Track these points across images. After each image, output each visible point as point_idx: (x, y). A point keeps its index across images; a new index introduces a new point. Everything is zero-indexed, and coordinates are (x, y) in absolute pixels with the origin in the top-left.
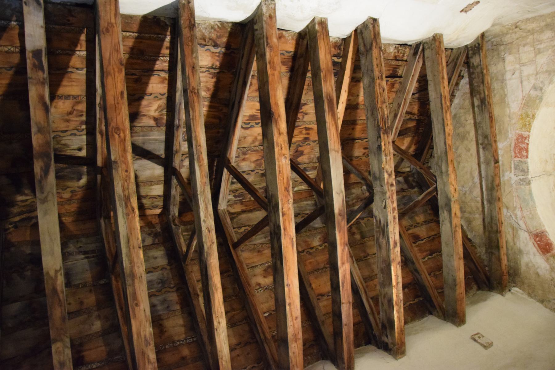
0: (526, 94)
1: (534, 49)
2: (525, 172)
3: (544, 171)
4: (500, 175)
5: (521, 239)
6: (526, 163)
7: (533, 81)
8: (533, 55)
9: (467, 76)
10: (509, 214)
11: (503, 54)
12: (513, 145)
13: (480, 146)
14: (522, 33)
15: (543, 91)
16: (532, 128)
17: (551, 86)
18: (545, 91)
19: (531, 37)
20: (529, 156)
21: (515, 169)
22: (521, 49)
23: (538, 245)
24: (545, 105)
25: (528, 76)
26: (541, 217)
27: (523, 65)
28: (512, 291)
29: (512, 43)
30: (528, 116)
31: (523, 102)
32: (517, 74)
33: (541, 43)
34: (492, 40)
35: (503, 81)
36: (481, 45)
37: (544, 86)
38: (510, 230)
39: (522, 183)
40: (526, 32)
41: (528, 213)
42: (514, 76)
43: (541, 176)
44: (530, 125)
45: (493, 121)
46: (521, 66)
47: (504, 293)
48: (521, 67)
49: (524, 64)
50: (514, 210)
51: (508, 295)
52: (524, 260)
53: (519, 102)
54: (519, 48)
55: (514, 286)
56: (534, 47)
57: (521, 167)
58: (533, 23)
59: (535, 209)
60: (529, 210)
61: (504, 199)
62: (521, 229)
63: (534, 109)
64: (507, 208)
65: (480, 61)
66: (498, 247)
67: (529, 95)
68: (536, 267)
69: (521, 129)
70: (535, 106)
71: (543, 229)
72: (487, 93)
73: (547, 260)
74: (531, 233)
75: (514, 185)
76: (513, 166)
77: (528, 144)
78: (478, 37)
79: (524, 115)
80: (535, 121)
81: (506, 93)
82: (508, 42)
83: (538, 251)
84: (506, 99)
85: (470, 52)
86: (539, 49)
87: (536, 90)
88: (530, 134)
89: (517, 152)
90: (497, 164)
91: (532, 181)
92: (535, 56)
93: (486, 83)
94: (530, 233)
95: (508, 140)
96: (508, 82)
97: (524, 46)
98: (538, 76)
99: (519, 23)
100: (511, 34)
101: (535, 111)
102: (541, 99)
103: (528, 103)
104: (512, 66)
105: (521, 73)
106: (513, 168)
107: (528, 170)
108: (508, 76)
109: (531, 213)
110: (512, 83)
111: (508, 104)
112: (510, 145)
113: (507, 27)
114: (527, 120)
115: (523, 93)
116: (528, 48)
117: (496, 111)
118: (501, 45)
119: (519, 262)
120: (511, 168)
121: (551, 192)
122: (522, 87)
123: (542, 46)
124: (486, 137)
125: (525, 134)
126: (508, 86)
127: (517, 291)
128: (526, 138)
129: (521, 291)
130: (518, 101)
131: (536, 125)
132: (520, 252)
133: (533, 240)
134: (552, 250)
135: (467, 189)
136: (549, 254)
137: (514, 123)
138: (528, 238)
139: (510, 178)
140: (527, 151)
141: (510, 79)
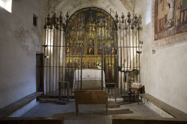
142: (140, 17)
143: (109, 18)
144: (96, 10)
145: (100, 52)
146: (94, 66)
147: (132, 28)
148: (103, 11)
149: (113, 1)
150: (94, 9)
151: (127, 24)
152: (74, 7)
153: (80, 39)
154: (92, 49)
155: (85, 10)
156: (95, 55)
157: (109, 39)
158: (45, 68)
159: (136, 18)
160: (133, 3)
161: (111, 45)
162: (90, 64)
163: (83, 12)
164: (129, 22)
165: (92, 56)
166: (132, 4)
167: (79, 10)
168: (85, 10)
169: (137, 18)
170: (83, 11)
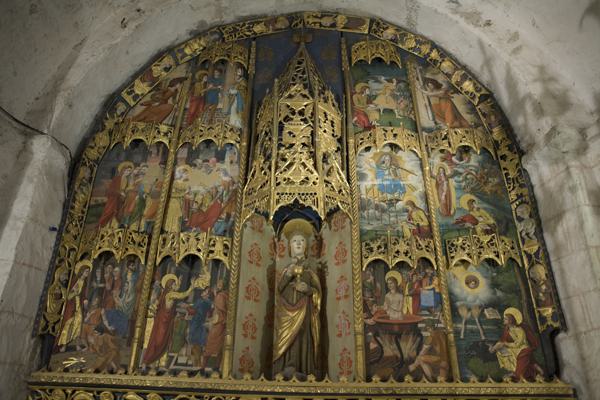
143: (441, 79)
144: (339, 28)
145: (389, 350)
153: (194, 219)
154: (307, 323)
157: (465, 224)
161: (494, 285)
168: (258, 29)
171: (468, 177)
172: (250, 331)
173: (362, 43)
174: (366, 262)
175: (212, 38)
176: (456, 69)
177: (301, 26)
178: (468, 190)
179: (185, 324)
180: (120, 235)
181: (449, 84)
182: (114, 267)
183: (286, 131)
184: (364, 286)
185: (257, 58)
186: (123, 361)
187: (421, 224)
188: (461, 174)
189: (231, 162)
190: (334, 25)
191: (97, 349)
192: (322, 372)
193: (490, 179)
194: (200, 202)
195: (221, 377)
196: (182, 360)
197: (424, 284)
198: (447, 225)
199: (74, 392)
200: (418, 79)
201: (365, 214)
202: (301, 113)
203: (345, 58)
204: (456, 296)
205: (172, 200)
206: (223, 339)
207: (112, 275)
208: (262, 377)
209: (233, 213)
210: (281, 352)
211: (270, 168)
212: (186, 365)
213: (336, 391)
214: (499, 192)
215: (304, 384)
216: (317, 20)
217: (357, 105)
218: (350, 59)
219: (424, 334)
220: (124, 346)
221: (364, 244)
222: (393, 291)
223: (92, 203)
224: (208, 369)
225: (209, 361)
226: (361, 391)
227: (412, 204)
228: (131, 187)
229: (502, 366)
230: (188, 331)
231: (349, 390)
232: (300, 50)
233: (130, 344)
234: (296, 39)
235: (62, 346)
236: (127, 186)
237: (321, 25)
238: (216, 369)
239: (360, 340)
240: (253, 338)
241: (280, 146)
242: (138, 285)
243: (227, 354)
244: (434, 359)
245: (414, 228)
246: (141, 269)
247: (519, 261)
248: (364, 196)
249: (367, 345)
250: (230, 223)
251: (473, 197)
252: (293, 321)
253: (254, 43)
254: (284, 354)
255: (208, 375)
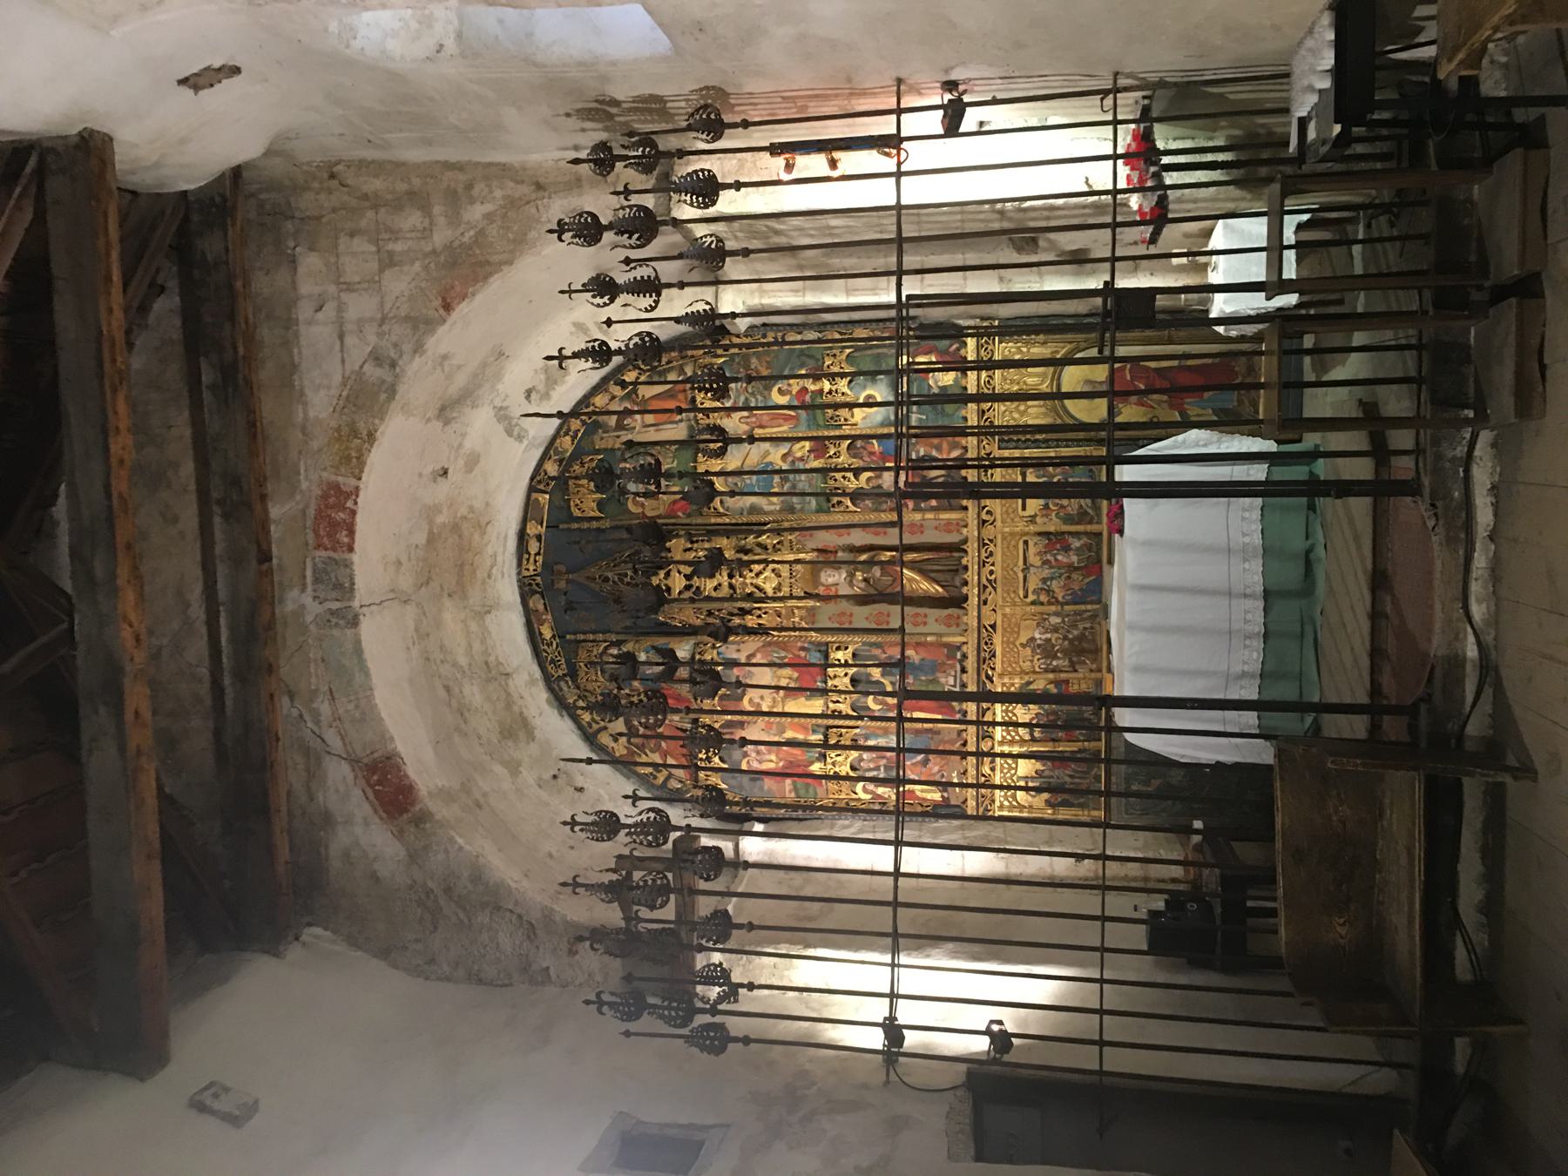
0: (352, 372)
1: (379, 251)
2: (345, 589)
3: (393, 591)
4: (273, 597)
5: (330, 783)
6: (348, 565)
7: (372, 339)
8: (375, 266)
9: (177, 290)
10: (295, 712)
11: (291, 244)
12: (311, 512)
13: (216, 509)
14: (346, 198)
15: (398, 370)
16: (366, 469)
17: (417, 359)
18: (403, 371)
19: (370, 214)
20: (357, 546)
21: (317, 581)
22: (343, 240)
23: (376, 793)
24: (402, 408)
25: (360, 323)
26: (384, 715)
27: (348, 290)
28: (304, 938)
29: (318, 218)
30: (355, 433)
31: (345, 394)
32: (329, 310)
33: (397, 239)
34: (262, 196)
35: (289, 323)
36: (229, 204)
37: (401, 356)
38: (299, 759)
39: (334, 620)
40: (358, 198)
41: (351, 707)
42: (320, 315)
43: (385, 604)
44: (361, 464)
45: (259, 436)
46: (341, 291)
47: (281, 948)
48: (342, 294)
49: (349, 288)
50: (311, 701)
51: (294, 952)
52: (340, 841)
53: (334, 392)
54: (337, 238)
55: (310, 925)
56: (378, 245)
57: (332, 575)
58: (377, 176)
59: (369, 693)
60: (352, 698)
61: (285, 670)
62: (329, 753)
63: (374, 417)
64: (292, 696)
65: (227, 250)
66: (265, 811)
67: (360, 373)
68: (372, 856)
69: (338, 468)
70: (376, 408)
71: (390, 747)
72: (241, 350)
73: (400, 835)
74: (358, 761)
75: (313, 628)
76: (309, 573)
77: (354, 513)
78: (223, 175)
79: (345, 430)
80: (373, 450)
81: (296, 358)
82: (308, 213)
83: (376, 811)
84: (295, 377)
85: (195, 218)
86: (391, 254)
87: (380, 366)
88: (362, 486)
89: (322, 533)
90: (265, 566)
91: (361, 617)
92: (381, 270)
93: (242, 321)
94: (354, 761)
95: (298, 498)
96: (303, 329)
97: (352, 235)
98: (386, 328)
99: (340, 167)
100: (317, 193)
101: (377, 421)
102: (392, 392)
103: (357, 397)
104: (316, 284)
105: (341, 308)
106: (309, 580)
107: (354, 584)
108: (304, 311)
109: (357, 707)
110: (315, 332)
111: (302, 394)
112: (304, 512)
113: (305, 168)
114: (353, 446)
115: (344, 370)
116: (361, 245)
117: (268, 407)
118: (287, 218)
119: (322, 850)
120: (304, 577)
121: (408, 648)
122: (342, 351)
123: (398, 247)
124: (235, 482)
125: (347, 482)
126: (303, 342)
127: (317, 937)
128: (348, 495)
129: (328, 933)
130: (329, 388)
131: (377, 458)
132: (327, 819)
133: (363, 781)
134: (413, 804)
135: (165, 642)
136: (405, 816)
137: (316, 448)
138: (350, 776)
139: (303, 606)
140: (351, 533)
141: (309, 323)
142: (601, 110)
146: (1076, 543)
147: (707, 189)
148: (552, 469)
149: (461, 380)
150: (534, 547)
151: (665, 240)
152: (517, 728)
155: (547, 633)
156: (972, 531)
158: (1117, 1061)
159: (603, 160)
160: (469, 187)
162: (1055, 585)
163: (570, 648)
164: (643, 226)
165: (982, 564)
166: (472, 201)
167: (551, 689)
168: (547, 633)
169: (603, 146)
170: (551, 651)
171: (750, 391)
172: (920, 619)
173: (572, 503)
174: (852, 508)
175: (565, 689)
176: (606, 391)
177: (539, 579)
178: (766, 393)
179: (918, 682)
180: (833, 755)
181: (622, 399)
182: (863, 760)
183: (714, 594)
184: (876, 510)
185: (594, 633)
186: (954, 736)
187: (807, 448)
188: (747, 399)
189: (738, 651)
190: (539, 537)
191: (943, 762)
192: (959, 548)
193: (753, 367)
194: (787, 681)
195: (966, 643)
196: (951, 681)
197: (873, 450)
198: (808, 421)
199: (983, 775)
200: (618, 437)
201: (798, 507)
202: (688, 577)
203: (595, 524)
204: (885, 420)
205: (787, 709)
206: (931, 644)
207: (871, 760)
208: (965, 605)
209: (799, 644)
210: (940, 589)
211: (759, 609)
212: (955, 677)
213: (976, 539)
214: (768, 359)
215: (970, 567)
216: (532, 559)
217: (661, 511)
218: (597, 519)
219: (922, 453)
220: (940, 737)
221: (832, 509)
222: (880, 482)
223: (793, 795)
224: (959, 656)
225: (951, 656)
226: (975, 516)
227: (784, 457)
228: (773, 757)
229: (951, 382)
230: (923, 678)
231: (976, 528)
232: (582, 580)
233: (938, 732)
234: (562, 585)
235: (942, 796)
236: (771, 761)
237: (538, 554)
238: (959, 648)
239: (929, 516)
240: (926, 616)
241: (731, 598)
242: (880, 732)
243: (945, 639)
244: (945, 446)
245: (812, 455)
246: (864, 732)
247: (848, 351)
248: (778, 508)
249: (933, 509)
250: (810, 646)
251: (775, 389)
252: (911, 580)
253: (568, 637)
254: (942, 586)
255: (965, 656)
